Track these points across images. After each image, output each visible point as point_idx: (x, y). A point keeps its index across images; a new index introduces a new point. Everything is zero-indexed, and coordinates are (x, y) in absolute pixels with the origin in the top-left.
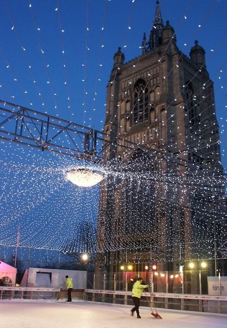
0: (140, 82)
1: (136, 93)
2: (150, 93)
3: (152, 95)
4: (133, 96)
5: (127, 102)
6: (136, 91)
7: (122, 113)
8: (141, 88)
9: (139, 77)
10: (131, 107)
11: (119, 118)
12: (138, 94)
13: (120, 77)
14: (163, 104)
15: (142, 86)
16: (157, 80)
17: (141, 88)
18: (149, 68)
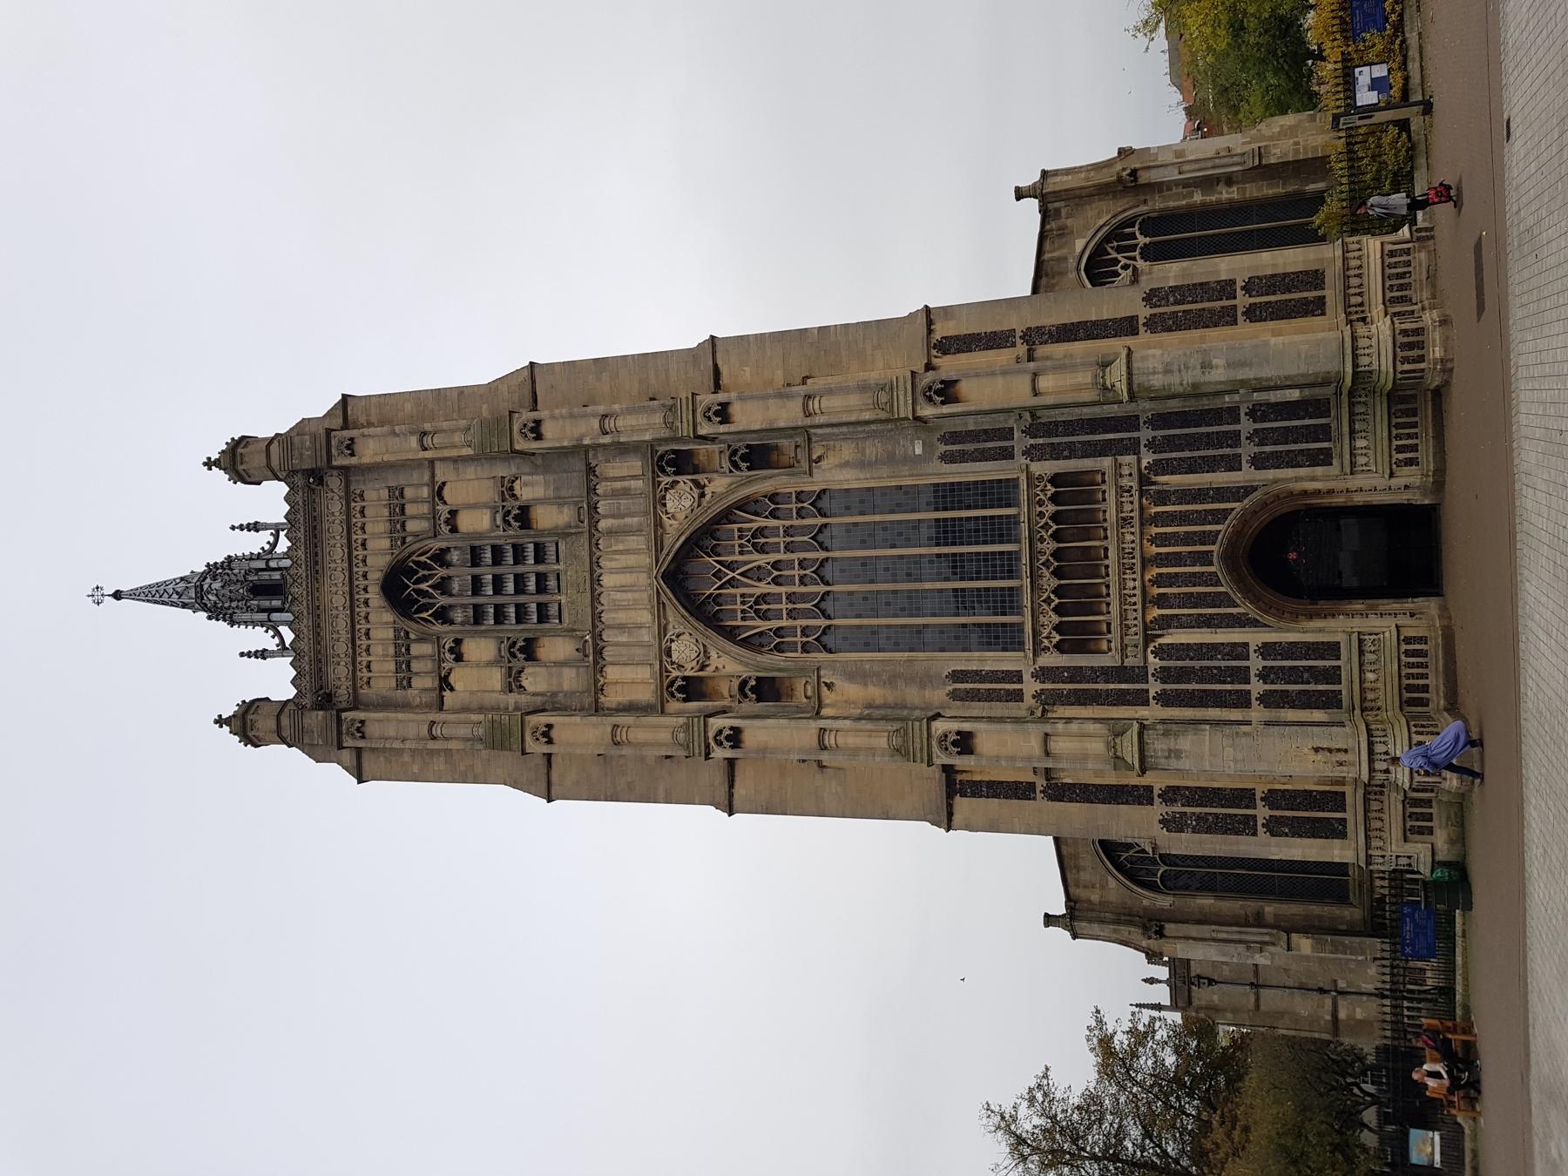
0: (399, 588)
1: (436, 615)
2: (454, 530)
3: (466, 522)
4: (446, 628)
5: (459, 658)
6: (424, 615)
7: (499, 688)
8: (424, 586)
9: (375, 596)
10: (483, 634)
11: (512, 699)
12: (443, 601)
13: (343, 694)
14: (516, 428)
15: (418, 581)
16: (414, 501)
17: (424, 586)
18: (358, 537)
